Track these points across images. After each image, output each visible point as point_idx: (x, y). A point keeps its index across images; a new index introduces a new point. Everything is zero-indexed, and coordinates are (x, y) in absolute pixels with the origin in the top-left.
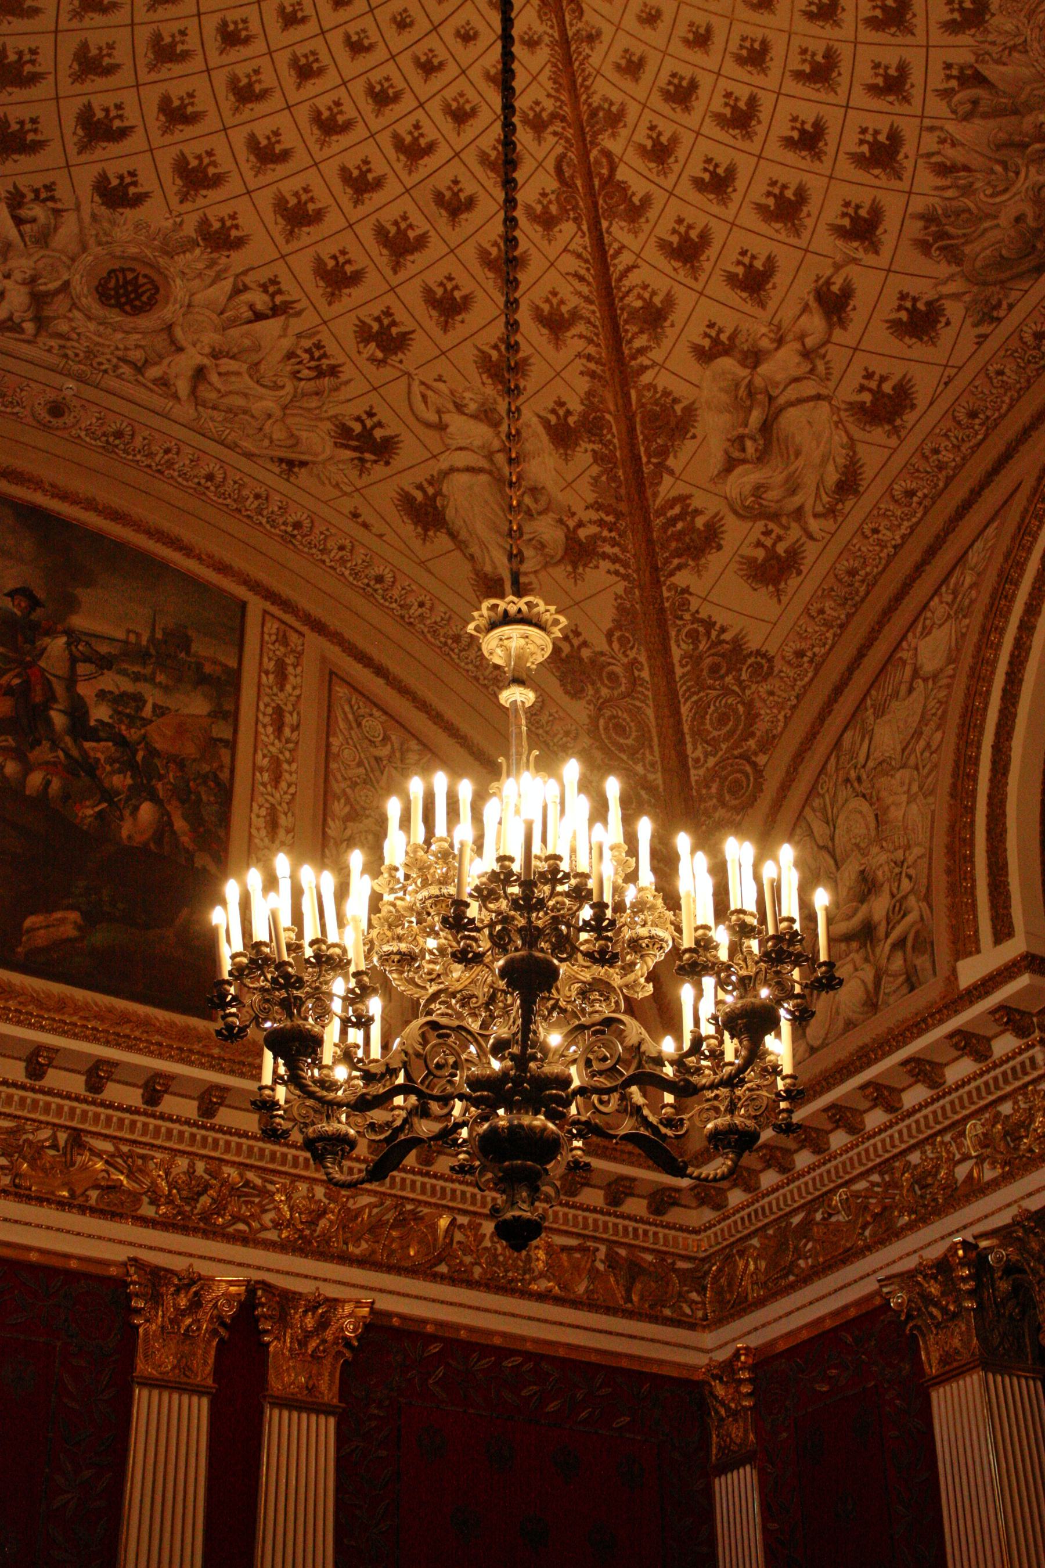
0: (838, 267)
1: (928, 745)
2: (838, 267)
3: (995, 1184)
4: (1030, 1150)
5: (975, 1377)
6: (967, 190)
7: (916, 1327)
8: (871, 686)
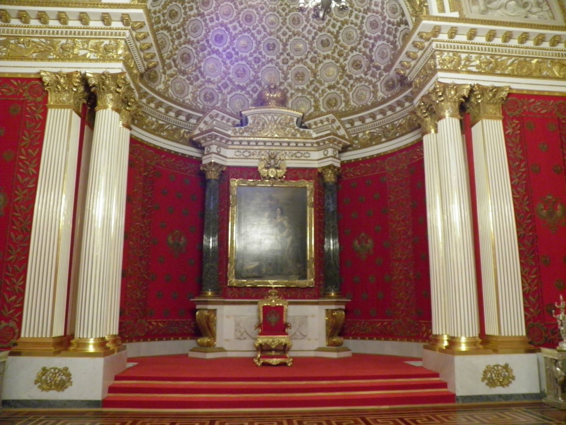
3: (96, 60)
4: (113, 57)
5: (69, 110)
7: (49, 89)
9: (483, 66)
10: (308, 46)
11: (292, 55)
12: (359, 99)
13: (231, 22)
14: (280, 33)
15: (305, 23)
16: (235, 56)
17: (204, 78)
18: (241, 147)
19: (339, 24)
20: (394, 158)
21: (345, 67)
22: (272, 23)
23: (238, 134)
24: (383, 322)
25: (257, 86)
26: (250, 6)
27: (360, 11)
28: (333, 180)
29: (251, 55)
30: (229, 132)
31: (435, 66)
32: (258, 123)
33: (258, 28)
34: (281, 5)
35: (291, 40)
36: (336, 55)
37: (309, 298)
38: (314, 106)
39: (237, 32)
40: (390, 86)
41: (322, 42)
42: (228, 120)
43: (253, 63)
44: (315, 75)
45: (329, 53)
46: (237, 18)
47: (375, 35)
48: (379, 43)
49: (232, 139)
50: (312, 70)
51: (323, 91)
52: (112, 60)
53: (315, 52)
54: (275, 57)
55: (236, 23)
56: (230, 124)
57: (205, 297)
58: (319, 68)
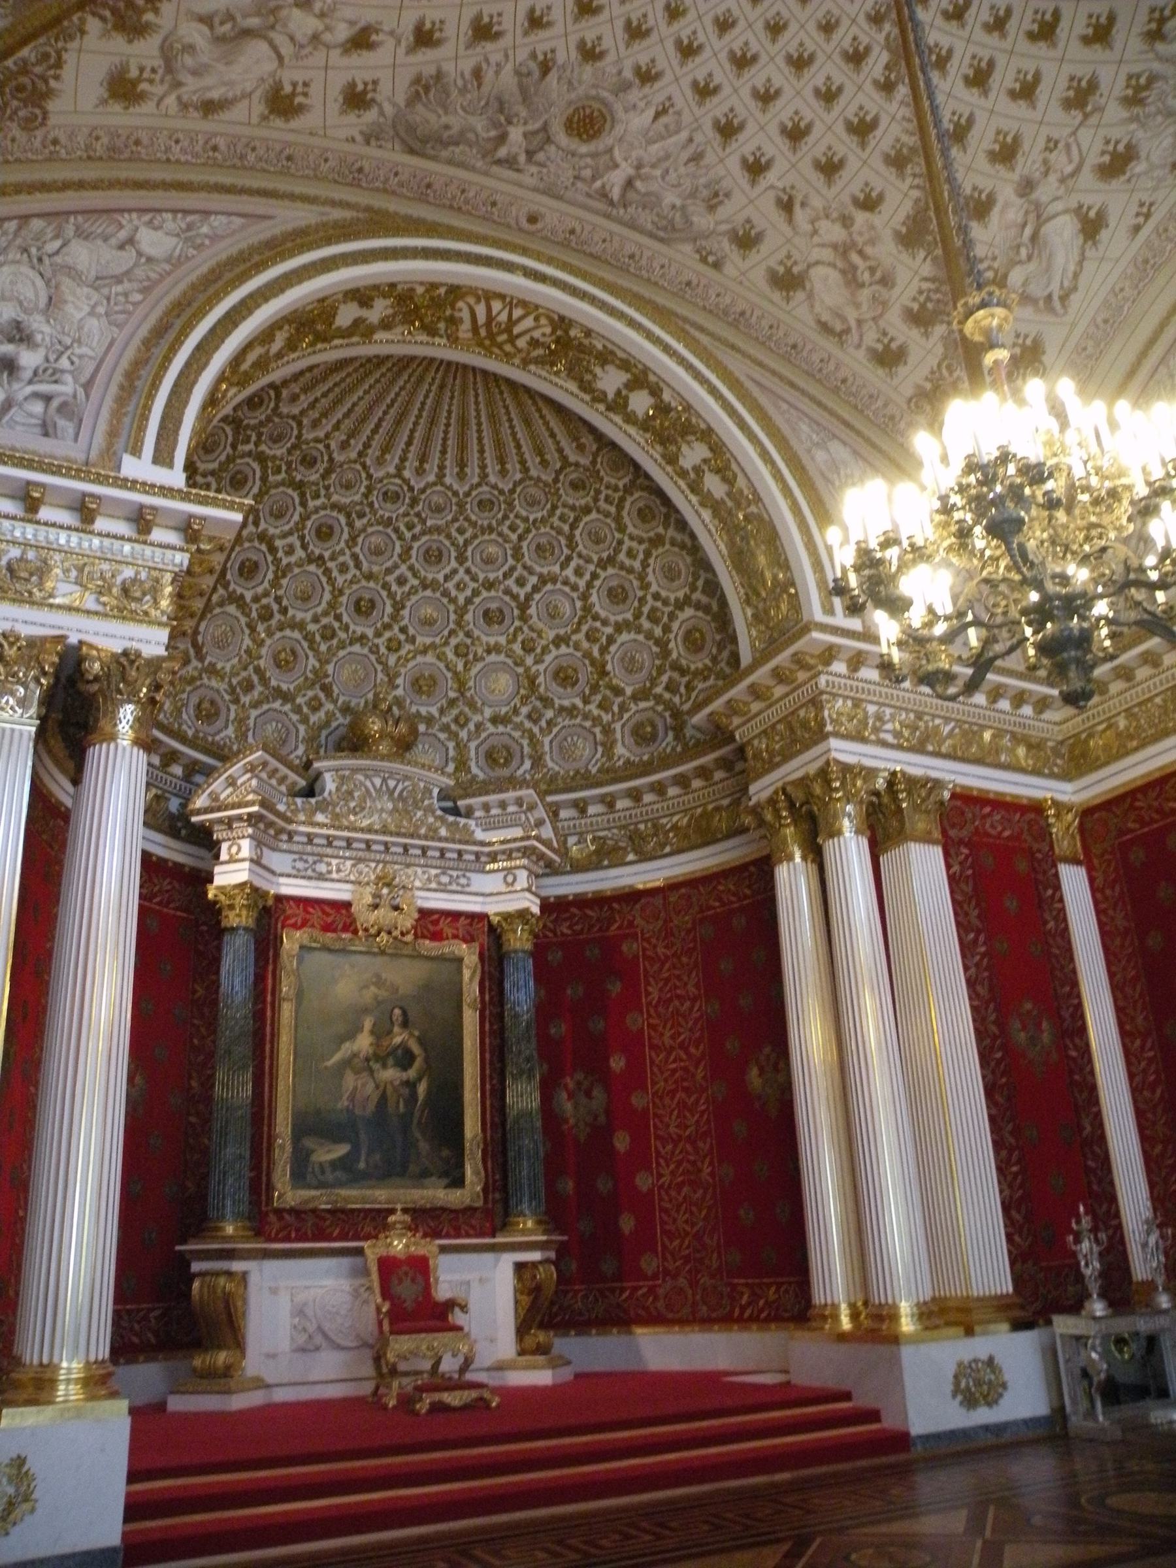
0: (392, 33)
1: (126, 295)
2: (392, 33)
6: (463, 91)
8: (83, 212)
9: (906, 733)
10: (453, 617)
11: (411, 631)
12: (565, 752)
13: (284, 536)
14: (390, 579)
15: (454, 564)
16: (277, 616)
17: (201, 659)
18: (309, 848)
19: (534, 580)
20: (658, 901)
21: (536, 677)
22: (377, 552)
23: (302, 817)
24: (636, 1289)
25: (322, 695)
26: (334, 506)
27: (588, 561)
28: (528, 946)
29: (316, 620)
30: (281, 808)
31: (822, 724)
32: (350, 793)
33: (341, 559)
34: (406, 514)
35: (414, 598)
36: (517, 647)
37: (468, 1236)
38: (454, 759)
39: (293, 559)
40: (642, 735)
41: (486, 613)
42: (282, 780)
43: (318, 638)
44: (462, 686)
45: (502, 640)
46: (299, 528)
47: (620, 618)
48: (624, 637)
49: (293, 827)
50: (456, 673)
51: (479, 726)
52: (145, 618)
53: (468, 634)
54: (370, 633)
55: (294, 539)
56: (283, 788)
57: (214, 1239)
58: (474, 671)
